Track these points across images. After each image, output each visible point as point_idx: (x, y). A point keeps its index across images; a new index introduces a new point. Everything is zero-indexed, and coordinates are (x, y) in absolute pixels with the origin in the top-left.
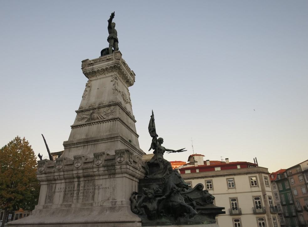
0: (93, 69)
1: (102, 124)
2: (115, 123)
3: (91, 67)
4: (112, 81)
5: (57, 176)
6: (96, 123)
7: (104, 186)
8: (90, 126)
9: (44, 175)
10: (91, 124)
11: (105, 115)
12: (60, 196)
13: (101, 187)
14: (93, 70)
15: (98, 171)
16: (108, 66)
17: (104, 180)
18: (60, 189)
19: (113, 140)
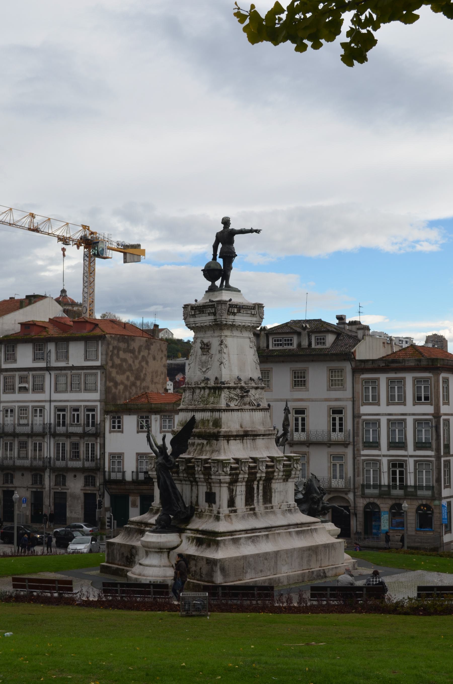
0: (234, 322)
1: (254, 412)
2: (267, 415)
3: (231, 317)
4: (251, 348)
5: (241, 478)
6: (248, 410)
7: (279, 490)
8: (242, 412)
9: (228, 477)
10: (244, 410)
11: (255, 400)
12: (242, 499)
13: (276, 490)
14: (234, 323)
15: (278, 475)
16: (250, 323)
17: (279, 484)
18: (240, 492)
19: (270, 437)
